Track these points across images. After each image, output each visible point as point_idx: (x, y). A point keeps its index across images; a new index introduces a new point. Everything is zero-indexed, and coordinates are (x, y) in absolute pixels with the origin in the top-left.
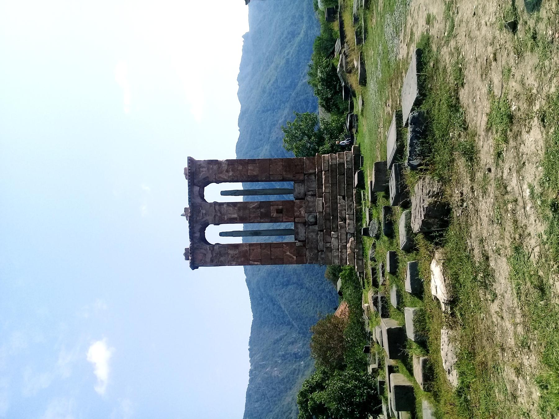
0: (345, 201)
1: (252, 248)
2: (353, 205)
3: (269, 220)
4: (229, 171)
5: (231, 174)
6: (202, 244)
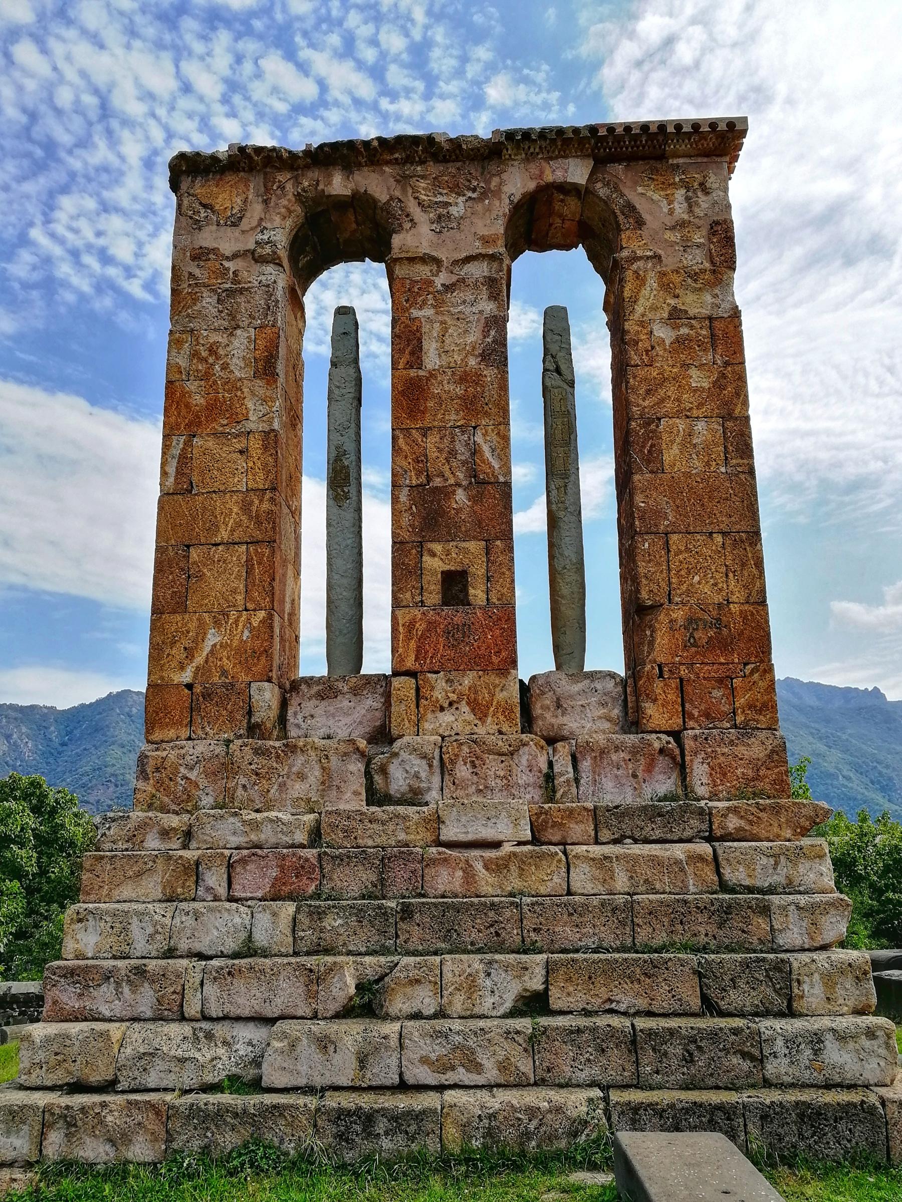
0: (513, 1013)
1: (255, 445)
2: (480, 1080)
3: (406, 536)
4: (676, 327)
5: (663, 333)
6: (290, 212)
